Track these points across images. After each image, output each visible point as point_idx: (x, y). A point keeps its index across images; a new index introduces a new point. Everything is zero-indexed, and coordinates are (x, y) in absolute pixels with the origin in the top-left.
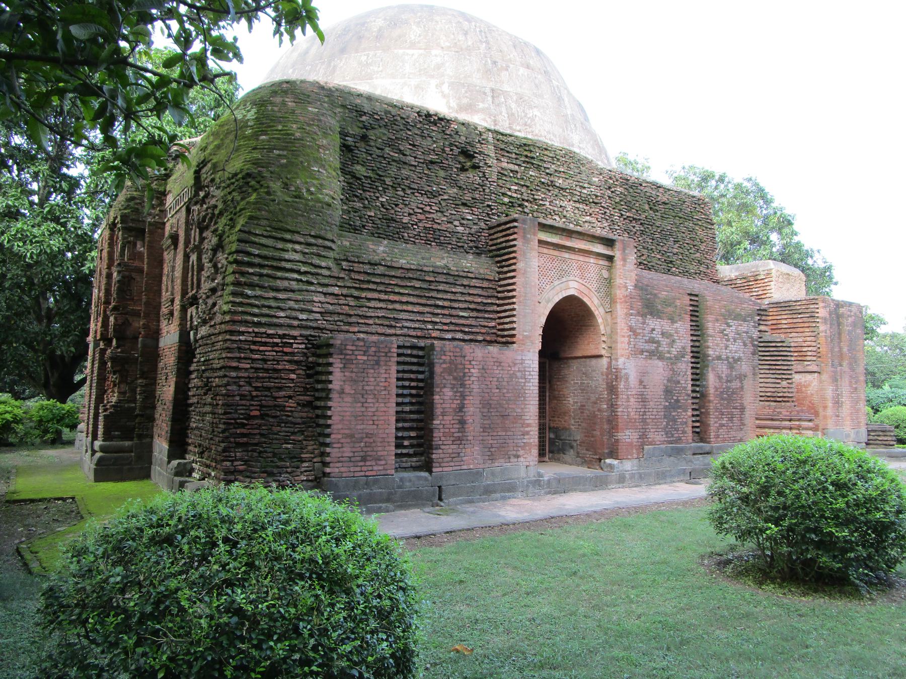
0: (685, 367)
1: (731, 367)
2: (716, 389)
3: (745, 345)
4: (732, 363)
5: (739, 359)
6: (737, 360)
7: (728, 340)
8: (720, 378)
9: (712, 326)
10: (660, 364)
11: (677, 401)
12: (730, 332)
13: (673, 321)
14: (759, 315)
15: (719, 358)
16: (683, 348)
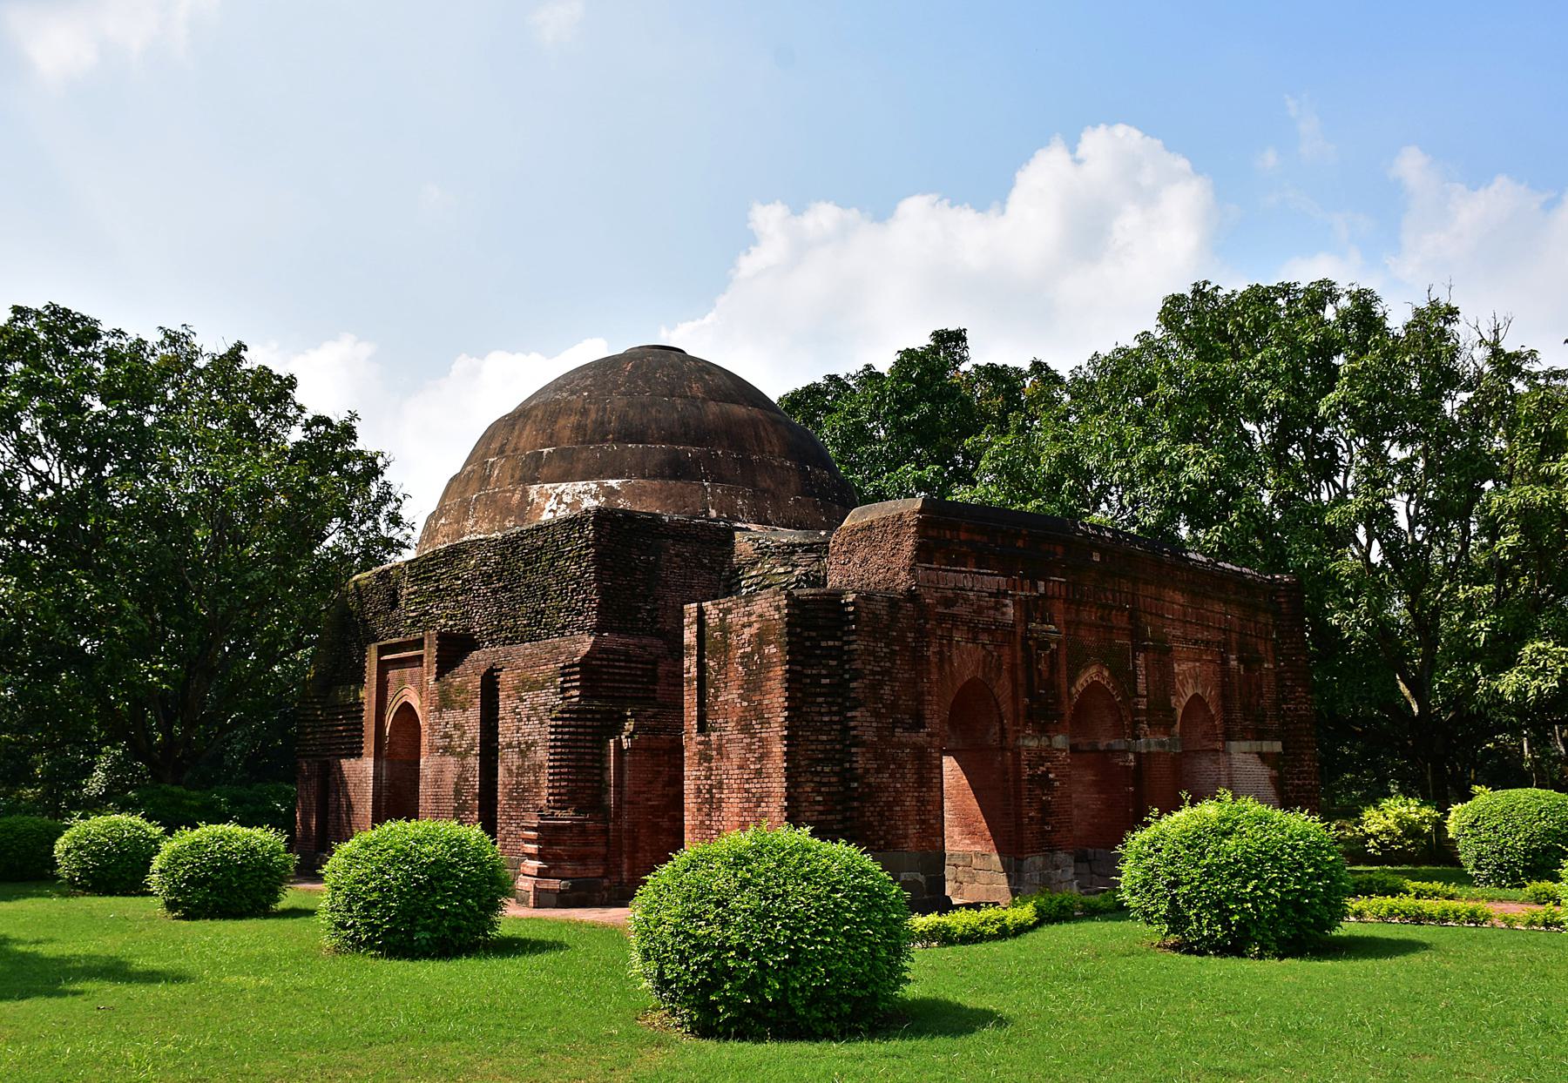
0: (474, 762)
1: (523, 754)
2: (505, 786)
3: (541, 723)
4: (525, 749)
5: (534, 743)
6: (529, 746)
7: (520, 720)
8: (509, 771)
9: (505, 705)
10: (452, 760)
11: (466, 801)
12: (524, 709)
13: (465, 710)
14: (563, 675)
15: (509, 745)
16: (473, 739)
